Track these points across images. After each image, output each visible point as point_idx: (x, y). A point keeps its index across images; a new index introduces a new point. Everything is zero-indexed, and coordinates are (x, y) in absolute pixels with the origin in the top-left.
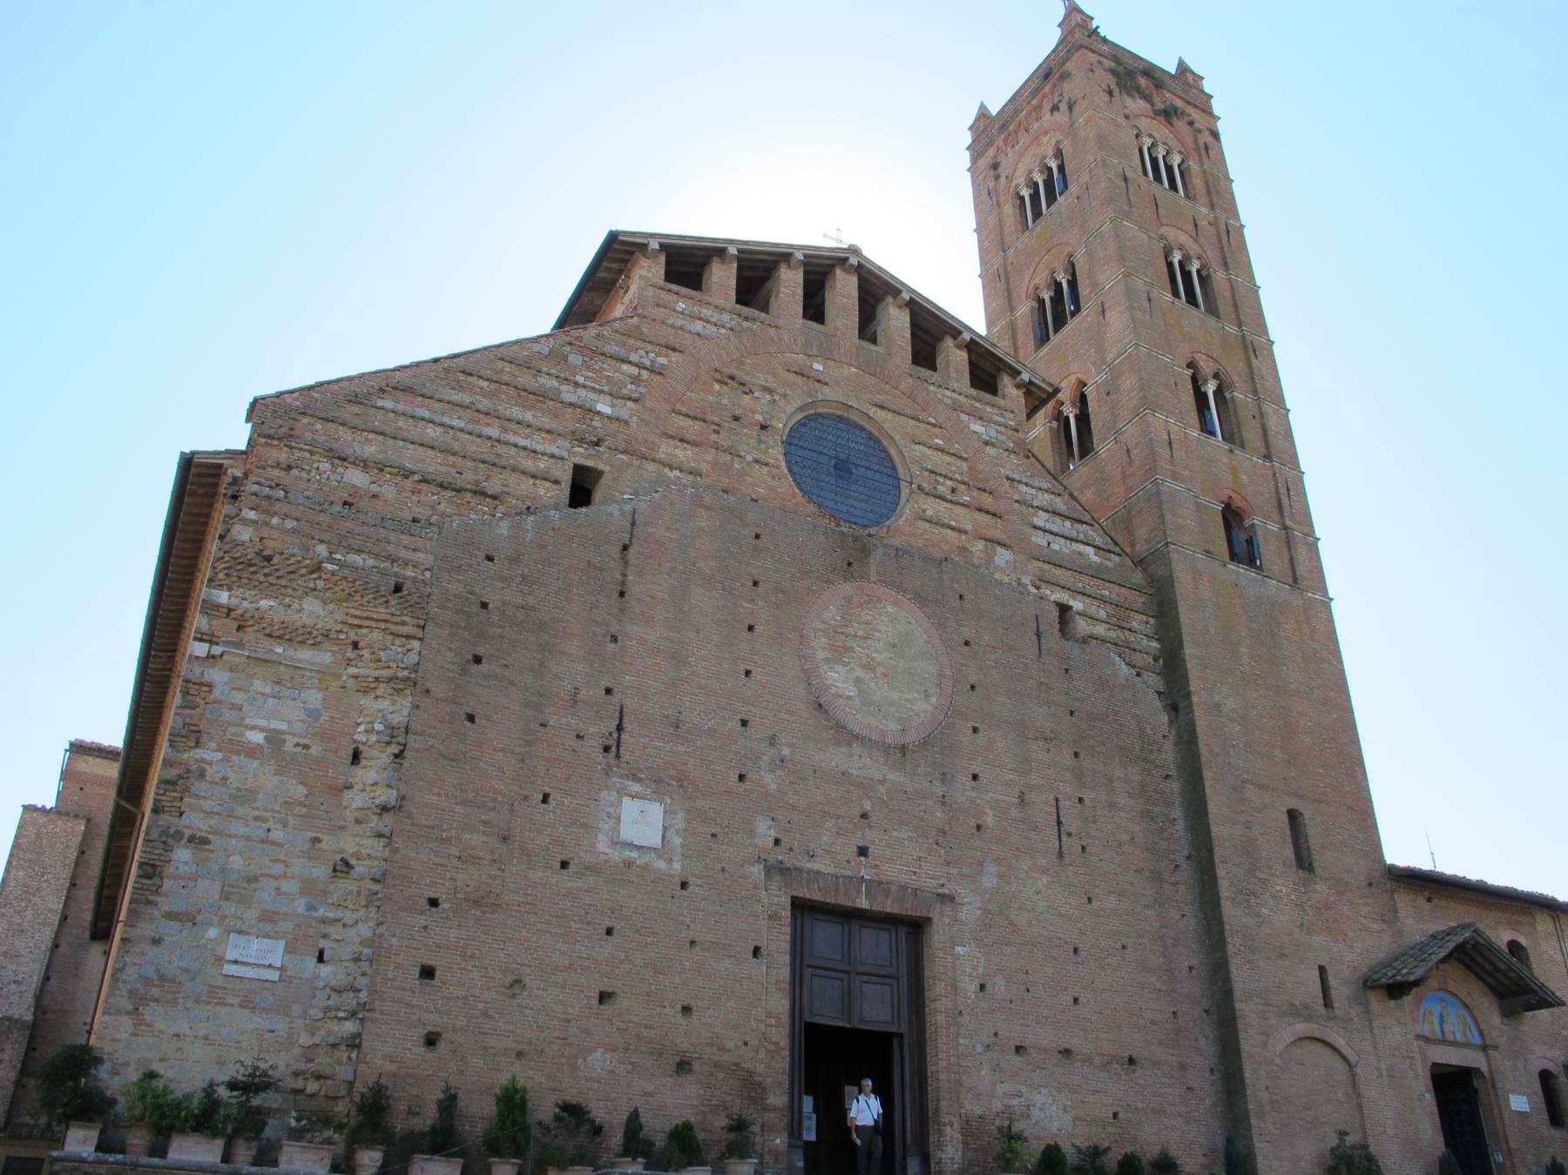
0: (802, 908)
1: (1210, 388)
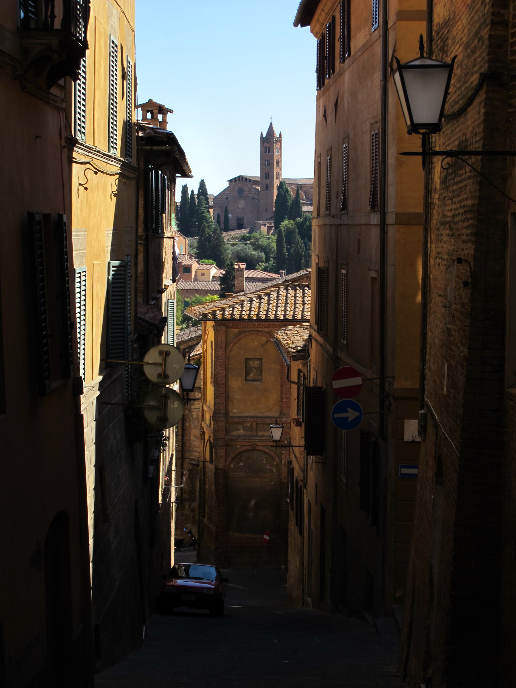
0: (237, 218)
1: (267, 174)
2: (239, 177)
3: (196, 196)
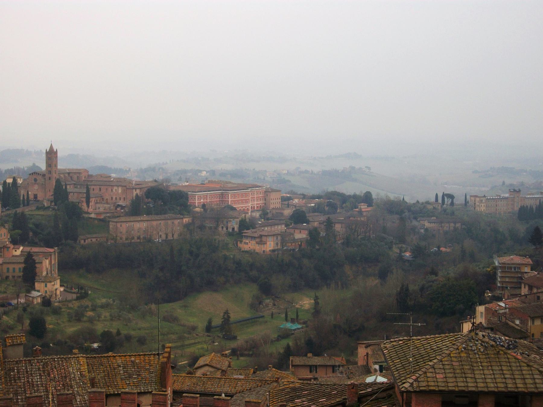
2: (34, 173)
3: (11, 186)
